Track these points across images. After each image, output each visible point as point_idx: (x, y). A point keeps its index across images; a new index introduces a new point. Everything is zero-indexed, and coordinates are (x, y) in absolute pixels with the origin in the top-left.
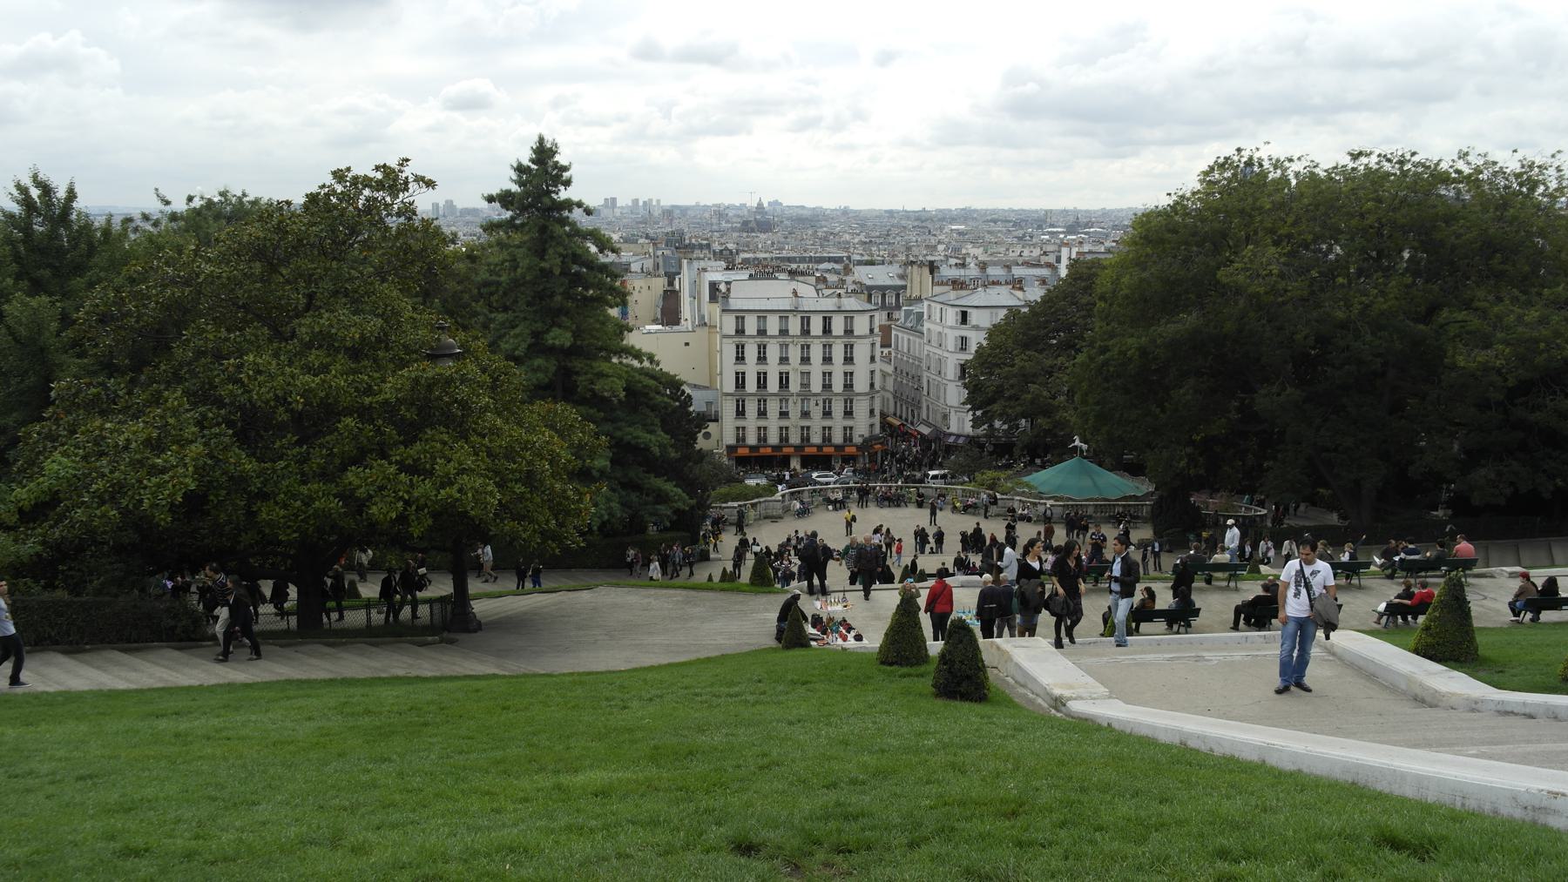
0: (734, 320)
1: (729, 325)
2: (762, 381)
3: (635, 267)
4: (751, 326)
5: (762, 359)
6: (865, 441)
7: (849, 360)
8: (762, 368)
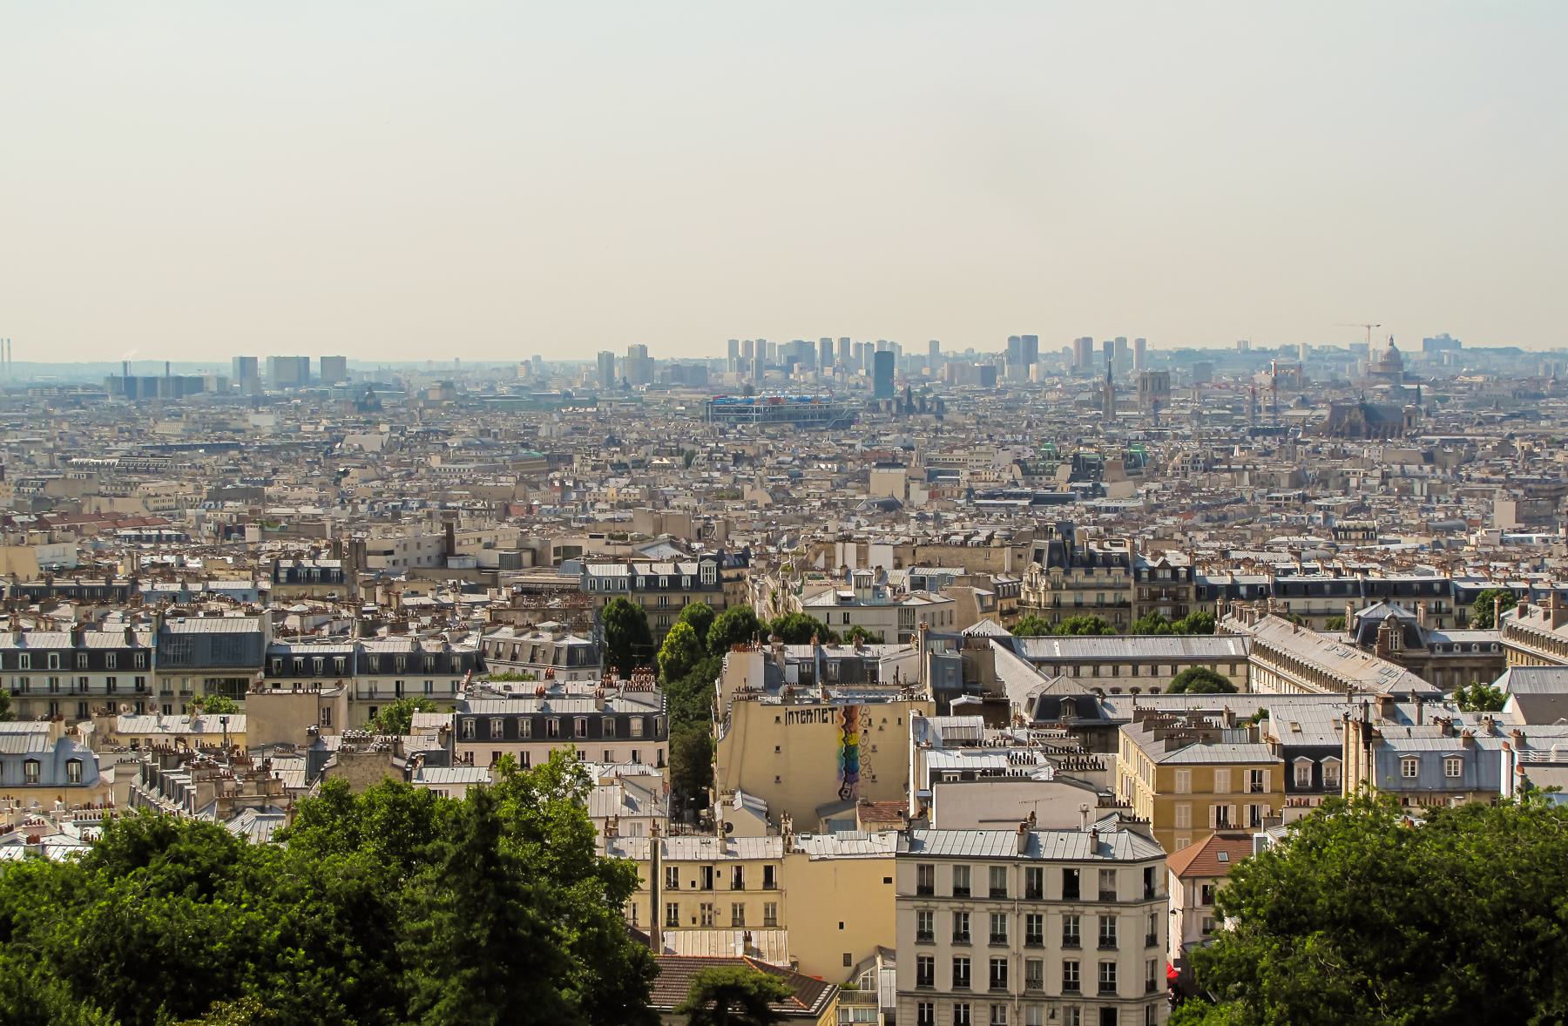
0: (915, 871)
1: (909, 880)
2: (962, 977)
3: (885, 674)
4: (944, 882)
5: (961, 937)
7: (1107, 942)
8: (962, 952)
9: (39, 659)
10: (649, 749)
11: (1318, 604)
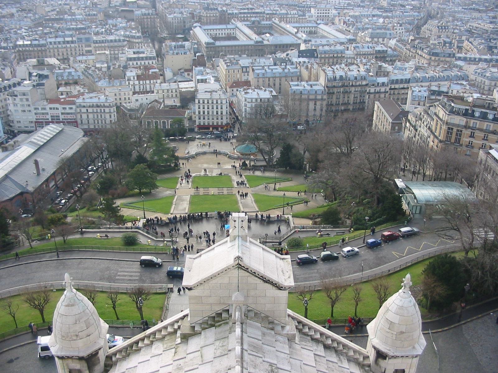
2: (204, 113)
3: (186, 48)
4: (201, 102)
5: (204, 108)
7: (222, 108)
8: (204, 110)
9: (59, 43)
10: (154, 62)
11: (245, 15)
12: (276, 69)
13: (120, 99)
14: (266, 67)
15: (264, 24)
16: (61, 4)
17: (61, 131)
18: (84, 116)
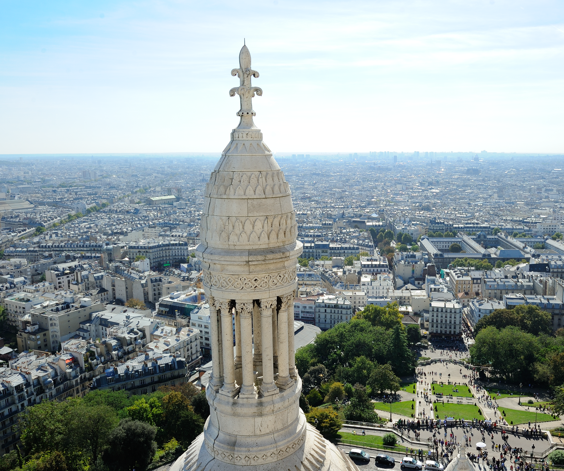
2: (437, 321)
3: (417, 258)
4: (435, 310)
6: (458, 334)
7: (455, 318)
12: (509, 282)
13: (355, 303)
14: (497, 280)
15: (490, 238)
16: (299, 214)
17: (302, 328)
18: (322, 316)
